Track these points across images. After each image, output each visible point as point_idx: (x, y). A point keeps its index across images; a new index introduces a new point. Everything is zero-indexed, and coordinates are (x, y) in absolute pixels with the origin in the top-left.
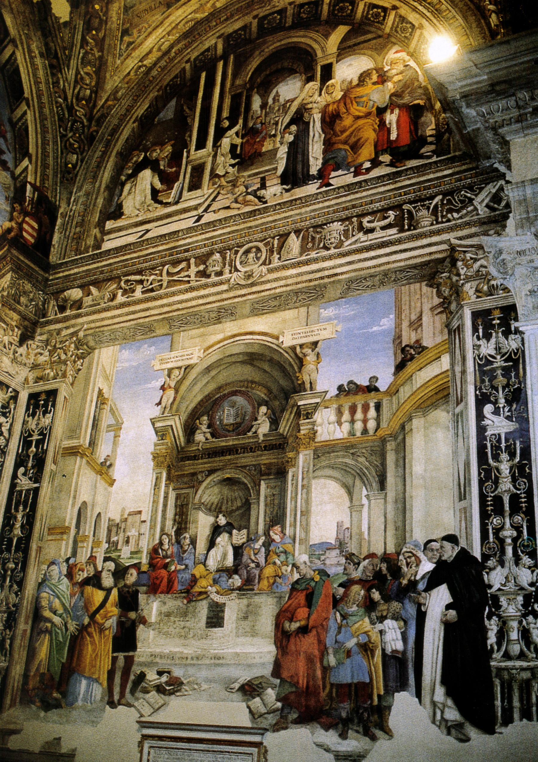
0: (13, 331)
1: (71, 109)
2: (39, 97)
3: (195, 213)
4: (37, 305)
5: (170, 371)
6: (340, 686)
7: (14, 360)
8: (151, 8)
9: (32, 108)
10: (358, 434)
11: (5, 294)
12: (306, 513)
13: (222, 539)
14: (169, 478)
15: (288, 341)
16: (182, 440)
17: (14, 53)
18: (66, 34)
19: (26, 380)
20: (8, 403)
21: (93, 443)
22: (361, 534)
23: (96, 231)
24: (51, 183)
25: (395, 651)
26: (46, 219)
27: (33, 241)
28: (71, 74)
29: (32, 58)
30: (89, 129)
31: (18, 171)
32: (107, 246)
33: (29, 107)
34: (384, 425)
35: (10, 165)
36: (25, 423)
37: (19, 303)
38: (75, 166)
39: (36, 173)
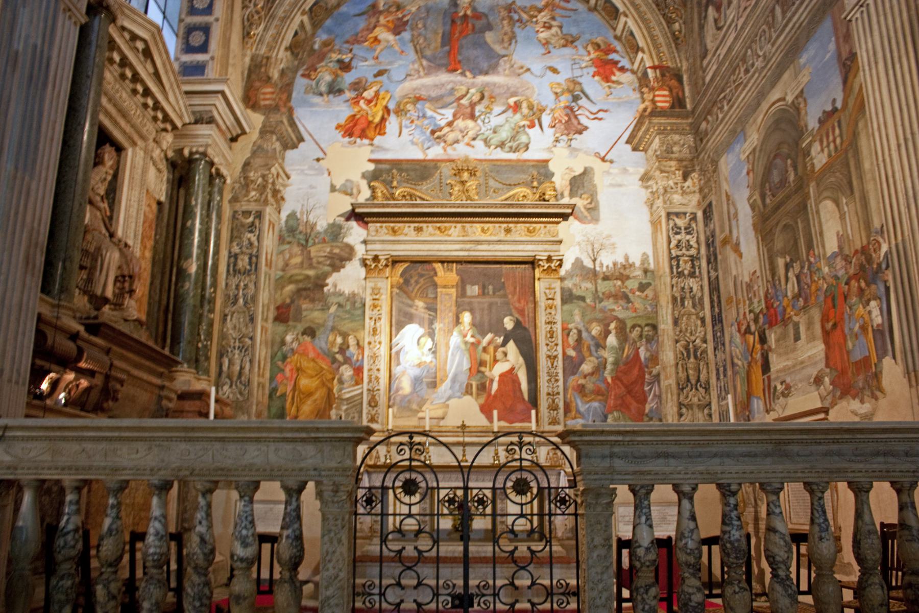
0: (675, 174)
3: (734, 25)
4: (689, 146)
5: (748, 157)
6: (856, 362)
7: (684, 193)
9: (630, 16)
10: (833, 154)
12: (821, 234)
13: (790, 274)
14: (762, 240)
15: (790, 99)
16: (761, 207)
19: (699, 202)
20: (689, 224)
21: (731, 231)
22: (848, 235)
23: (701, 73)
24: (667, 55)
25: (878, 325)
26: (674, 83)
27: (667, 105)
31: (636, 66)
32: (708, 79)
33: (626, 16)
34: (845, 138)
36: (705, 232)
37: (672, 153)
39: (652, 57)
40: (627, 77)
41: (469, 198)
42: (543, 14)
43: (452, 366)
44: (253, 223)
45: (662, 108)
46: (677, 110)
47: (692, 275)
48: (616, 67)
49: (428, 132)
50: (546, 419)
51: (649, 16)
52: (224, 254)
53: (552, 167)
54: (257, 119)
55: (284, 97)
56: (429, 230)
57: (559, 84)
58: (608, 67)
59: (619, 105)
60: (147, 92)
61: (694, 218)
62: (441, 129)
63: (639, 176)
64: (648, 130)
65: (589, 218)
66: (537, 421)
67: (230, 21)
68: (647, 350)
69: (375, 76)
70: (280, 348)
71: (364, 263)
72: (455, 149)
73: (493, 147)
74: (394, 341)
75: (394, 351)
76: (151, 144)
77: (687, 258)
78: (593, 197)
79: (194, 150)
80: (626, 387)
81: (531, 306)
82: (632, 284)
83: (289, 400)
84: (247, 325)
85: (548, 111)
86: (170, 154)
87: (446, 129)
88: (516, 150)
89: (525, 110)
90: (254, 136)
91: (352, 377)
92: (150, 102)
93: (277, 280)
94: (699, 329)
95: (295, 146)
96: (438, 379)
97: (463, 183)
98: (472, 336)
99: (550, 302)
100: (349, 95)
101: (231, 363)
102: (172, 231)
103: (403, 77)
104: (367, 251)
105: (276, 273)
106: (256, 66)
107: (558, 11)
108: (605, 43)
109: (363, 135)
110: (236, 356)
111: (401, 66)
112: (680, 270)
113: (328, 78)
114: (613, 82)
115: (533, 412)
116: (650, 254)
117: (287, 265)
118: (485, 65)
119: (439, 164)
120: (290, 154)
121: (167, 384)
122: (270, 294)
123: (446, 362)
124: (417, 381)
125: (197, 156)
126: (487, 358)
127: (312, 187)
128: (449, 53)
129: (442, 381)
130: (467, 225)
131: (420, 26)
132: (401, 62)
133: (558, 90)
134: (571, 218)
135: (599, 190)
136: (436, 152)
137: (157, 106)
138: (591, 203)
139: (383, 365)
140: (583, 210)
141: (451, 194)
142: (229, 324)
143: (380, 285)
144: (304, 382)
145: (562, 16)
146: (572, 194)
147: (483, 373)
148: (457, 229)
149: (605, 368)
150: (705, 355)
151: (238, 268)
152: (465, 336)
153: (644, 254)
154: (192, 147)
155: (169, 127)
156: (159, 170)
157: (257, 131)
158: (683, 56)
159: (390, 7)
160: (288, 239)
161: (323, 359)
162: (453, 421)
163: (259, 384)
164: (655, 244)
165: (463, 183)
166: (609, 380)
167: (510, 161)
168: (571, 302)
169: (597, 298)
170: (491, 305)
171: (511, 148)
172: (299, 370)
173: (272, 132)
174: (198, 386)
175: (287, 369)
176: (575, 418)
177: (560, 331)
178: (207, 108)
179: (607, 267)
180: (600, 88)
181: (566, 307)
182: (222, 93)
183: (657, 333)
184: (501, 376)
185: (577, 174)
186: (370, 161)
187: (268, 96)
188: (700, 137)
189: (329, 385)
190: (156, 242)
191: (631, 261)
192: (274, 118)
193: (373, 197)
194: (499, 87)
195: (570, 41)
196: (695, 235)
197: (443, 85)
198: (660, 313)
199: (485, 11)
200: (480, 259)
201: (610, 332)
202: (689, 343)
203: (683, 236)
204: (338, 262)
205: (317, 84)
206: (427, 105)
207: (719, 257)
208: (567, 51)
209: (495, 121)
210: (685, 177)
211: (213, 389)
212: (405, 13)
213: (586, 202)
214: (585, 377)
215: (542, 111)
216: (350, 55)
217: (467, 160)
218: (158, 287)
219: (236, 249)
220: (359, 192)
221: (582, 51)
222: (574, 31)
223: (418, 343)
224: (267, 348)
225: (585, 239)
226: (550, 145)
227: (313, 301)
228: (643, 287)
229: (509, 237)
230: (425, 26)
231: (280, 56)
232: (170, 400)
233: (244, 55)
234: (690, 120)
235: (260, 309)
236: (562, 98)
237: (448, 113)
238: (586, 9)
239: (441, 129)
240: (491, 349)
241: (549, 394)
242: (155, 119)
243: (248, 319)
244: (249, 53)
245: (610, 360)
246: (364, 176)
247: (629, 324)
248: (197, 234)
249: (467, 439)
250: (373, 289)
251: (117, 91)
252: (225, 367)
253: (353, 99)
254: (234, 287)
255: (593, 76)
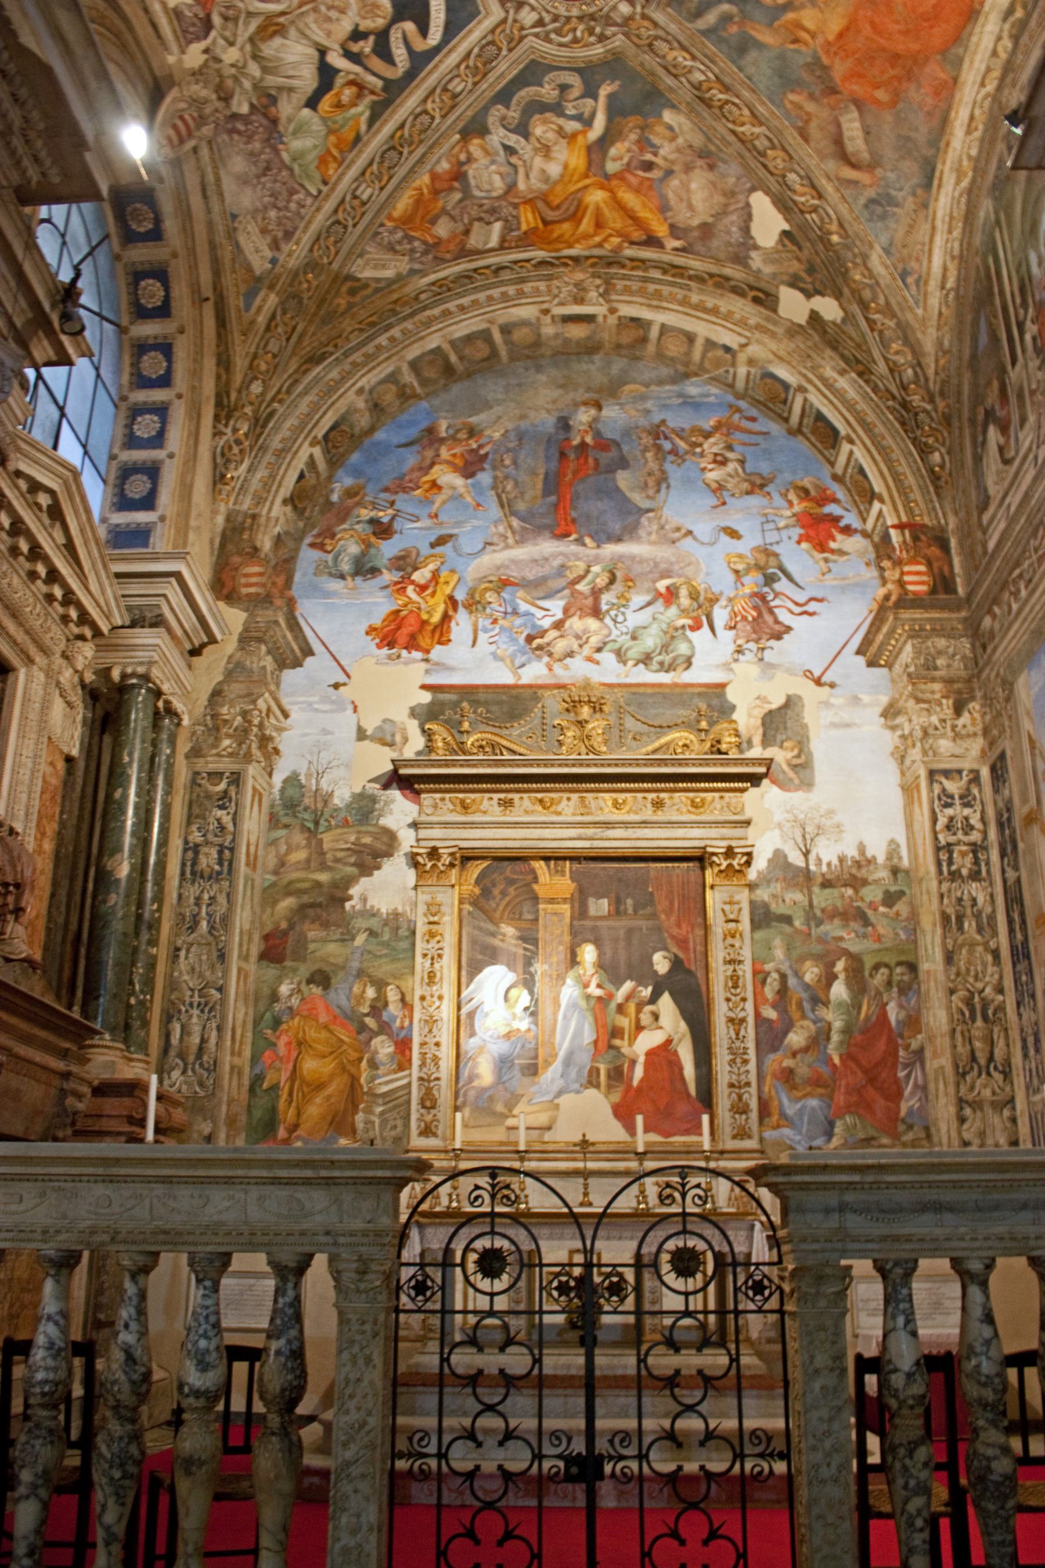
0: (940, 704)
1: (905, 405)
2: (862, 422)
4: (964, 657)
7: (957, 736)
8: (911, 226)
11: (912, 669)
17: (806, 400)
18: (849, 329)
19: (983, 751)
20: (968, 789)
23: (979, 535)
26: (935, 551)
27: (923, 588)
28: (882, 367)
29: (829, 386)
30: (936, 410)
31: (869, 526)
32: (991, 545)
33: (851, 442)
35: (856, 524)
37: (936, 668)
38: (942, 466)
40: (854, 544)
41: (591, 750)
42: (712, 440)
43: (564, 1038)
44: (226, 792)
45: (914, 593)
46: (942, 596)
47: (975, 876)
48: (836, 527)
49: (522, 639)
50: (728, 1131)
51: (889, 441)
52: (176, 844)
53: (732, 695)
54: (235, 618)
55: (280, 580)
56: (525, 804)
57: (740, 556)
58: (822, 526)
59: (843, 590)
60: (53, 576)
61: (975, 778)
62: (543, 633)
63: (879, 710)
64: (892, 631)
65: (797, 781)
66: (712, 1133)
67: (192, 458)
68: (901, 1006)
69: (433, 546)
70: (269, 1007)
71: (413, 861)
72: (567, 668)
73: (630, 663)
74: (464, 994)
75: (465, 1010)
76: (58, 661)
77: (964, 848)
78: (802, 745)
79: (129, 670)
80: (866, 1071)
81: (699, 932)
82: (872, 894)
83: (284, 1096)
84: (213, 967)
85: (723, 602)
86: (89, 677)
87: (553, 634)
88: (670, 668)
89: (685, 601)
90: (230, 646)
91: (392, 1057)
92: (58, 592)
93: (264, 890)
94: (990, 969)
95: (297, 664)
96: (540, 1061)
97: (581, 724)
98: (599, 986)
99: (732, 925)
100: (388, 577)
101: (185, 1031)
102: (88, 805)
103: (480, 546)
104: (418, 840)
105: (264, 878)
106: (234, 530)
107: (738, 436)
108: (816, 486)
109: (412, 644)
110: (195, 1020)
111: (475, 528)
112: (954, 868)
113: (354, 549)
114: (832, 551)
115: (705, 1118)
116: (902, 841)
117: (282, 864)
118: (616, 527)
119: (540, 692)
120: (289, 676)
121: (74, 1069)
122: (254, 913)
123: (553, 1030)
124: (503, 1064)
125: (134, 681)
126: (624, 1022)
127: (326, 732)
128: (556, 506)
129: (548, 1064)
130: (589, 796)
131: (507, 462)
132: (475, 522)
133: (740, 567)
134: (765, 782)
135: (812, 734)
136: (534, 672)
137: (69, 599)
138: (798, 756)
139: (445, 1035)
140: (785, 768)
141: (561, 743)
142: (183, 964)
143: (440, 898)
144: (310, 1065)
145: (744, 444)
146: (766, 743)
147: (617, 1049)
148: (572, 803)
149: (828, 1039)
150: (1001, 1015)
151: (198, 868)
152: (586, 986)
153: (892, 841)
154: (125, 665)
155: (88, 632)
156: (69, 704)
157: (235, 637)
158: (948, 510)
159: (458, 431)
160: (286, 820)
161: (343, 1026)
162: (566, 1134)
163: (232, 1068)
164: (909, 825)
165: (581, 724)
166: (837, 1060)
167: (660, 685)
168: (768, 926)
169: (811, 916)
170: (630, 932)
171: (661, 664)
172: (301, 1044)
173: (260, 640)
174: (129, 1072)
175: (282, 1043)
176: (778, 1127)
177: (749, 976)
178: (153, 601)
179: (829, 864)
180: (810, 562)
181: (759, 935)
182: (178, 575)
183: (917, 977)
184: (650, 1054)
185: (774, 706)
186: (424, 687)
187: (254, 580)
188: (982, 641)
189: (353, 1071)
190: (62, 824)
191: (869, 854)
192: (264, 616)
193: (430, 748)
194: (641, 562)
195: (757, 485)
196: (978, 808)
197: (546, 559)
198: (921, 942)
199: (617, 437)
200: (612, 853)
201: (835, 977)
202: (972, 994)
203: (957, 811)
204: (368, 859)
205: (336, 559)
206: (521, 593)
207: (1021, 846)
208: (755, 501)
209: (634, 619)
210: (958, 710)
211: (154, 1078)
212: (482, 441)
213: (790, 755)
214: (794, 1055)
215: (713, 601)
216: (390, 512)
217: (587, 685)
218: (64, 900)
219: (196, 837)
220: (406, 740)
221: (778, 501)
222: (765, 468)
223: (506, 999)
224: (246, 1005)
225: (790, 817)
226: (729, 659)
227: (326, 925)
228: (890, 899)
229: (660, 816)
230: (515, 462)
231: (273, 514)
232: (79, 1096)
233: (215, 512)
234: (964, 614)
235: (237, 939)
236: (746, 580)
237: (556, 607)
238: (784, 432)
239: (543, 633)
240: (632, 1008)
241: (731, 1085)
242: (65, 619)
243: (215, 954)
244: (222, 508)
245: (837, 1025)
246: (413, 713)
247: (869, 963)
248: (130, 812)
249: (591, 1165)
250: (429, 905)
251: (5, 574)
252: (175, 1040)
253: (396, 583)
254: (192, 900)
255: (799, 542)
